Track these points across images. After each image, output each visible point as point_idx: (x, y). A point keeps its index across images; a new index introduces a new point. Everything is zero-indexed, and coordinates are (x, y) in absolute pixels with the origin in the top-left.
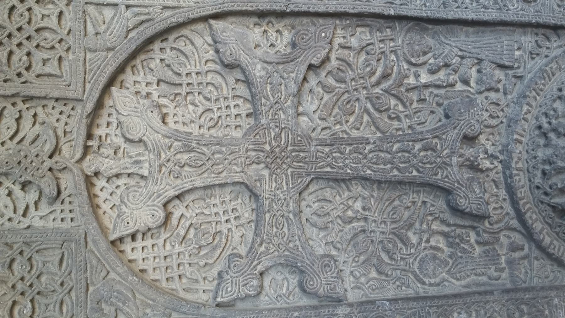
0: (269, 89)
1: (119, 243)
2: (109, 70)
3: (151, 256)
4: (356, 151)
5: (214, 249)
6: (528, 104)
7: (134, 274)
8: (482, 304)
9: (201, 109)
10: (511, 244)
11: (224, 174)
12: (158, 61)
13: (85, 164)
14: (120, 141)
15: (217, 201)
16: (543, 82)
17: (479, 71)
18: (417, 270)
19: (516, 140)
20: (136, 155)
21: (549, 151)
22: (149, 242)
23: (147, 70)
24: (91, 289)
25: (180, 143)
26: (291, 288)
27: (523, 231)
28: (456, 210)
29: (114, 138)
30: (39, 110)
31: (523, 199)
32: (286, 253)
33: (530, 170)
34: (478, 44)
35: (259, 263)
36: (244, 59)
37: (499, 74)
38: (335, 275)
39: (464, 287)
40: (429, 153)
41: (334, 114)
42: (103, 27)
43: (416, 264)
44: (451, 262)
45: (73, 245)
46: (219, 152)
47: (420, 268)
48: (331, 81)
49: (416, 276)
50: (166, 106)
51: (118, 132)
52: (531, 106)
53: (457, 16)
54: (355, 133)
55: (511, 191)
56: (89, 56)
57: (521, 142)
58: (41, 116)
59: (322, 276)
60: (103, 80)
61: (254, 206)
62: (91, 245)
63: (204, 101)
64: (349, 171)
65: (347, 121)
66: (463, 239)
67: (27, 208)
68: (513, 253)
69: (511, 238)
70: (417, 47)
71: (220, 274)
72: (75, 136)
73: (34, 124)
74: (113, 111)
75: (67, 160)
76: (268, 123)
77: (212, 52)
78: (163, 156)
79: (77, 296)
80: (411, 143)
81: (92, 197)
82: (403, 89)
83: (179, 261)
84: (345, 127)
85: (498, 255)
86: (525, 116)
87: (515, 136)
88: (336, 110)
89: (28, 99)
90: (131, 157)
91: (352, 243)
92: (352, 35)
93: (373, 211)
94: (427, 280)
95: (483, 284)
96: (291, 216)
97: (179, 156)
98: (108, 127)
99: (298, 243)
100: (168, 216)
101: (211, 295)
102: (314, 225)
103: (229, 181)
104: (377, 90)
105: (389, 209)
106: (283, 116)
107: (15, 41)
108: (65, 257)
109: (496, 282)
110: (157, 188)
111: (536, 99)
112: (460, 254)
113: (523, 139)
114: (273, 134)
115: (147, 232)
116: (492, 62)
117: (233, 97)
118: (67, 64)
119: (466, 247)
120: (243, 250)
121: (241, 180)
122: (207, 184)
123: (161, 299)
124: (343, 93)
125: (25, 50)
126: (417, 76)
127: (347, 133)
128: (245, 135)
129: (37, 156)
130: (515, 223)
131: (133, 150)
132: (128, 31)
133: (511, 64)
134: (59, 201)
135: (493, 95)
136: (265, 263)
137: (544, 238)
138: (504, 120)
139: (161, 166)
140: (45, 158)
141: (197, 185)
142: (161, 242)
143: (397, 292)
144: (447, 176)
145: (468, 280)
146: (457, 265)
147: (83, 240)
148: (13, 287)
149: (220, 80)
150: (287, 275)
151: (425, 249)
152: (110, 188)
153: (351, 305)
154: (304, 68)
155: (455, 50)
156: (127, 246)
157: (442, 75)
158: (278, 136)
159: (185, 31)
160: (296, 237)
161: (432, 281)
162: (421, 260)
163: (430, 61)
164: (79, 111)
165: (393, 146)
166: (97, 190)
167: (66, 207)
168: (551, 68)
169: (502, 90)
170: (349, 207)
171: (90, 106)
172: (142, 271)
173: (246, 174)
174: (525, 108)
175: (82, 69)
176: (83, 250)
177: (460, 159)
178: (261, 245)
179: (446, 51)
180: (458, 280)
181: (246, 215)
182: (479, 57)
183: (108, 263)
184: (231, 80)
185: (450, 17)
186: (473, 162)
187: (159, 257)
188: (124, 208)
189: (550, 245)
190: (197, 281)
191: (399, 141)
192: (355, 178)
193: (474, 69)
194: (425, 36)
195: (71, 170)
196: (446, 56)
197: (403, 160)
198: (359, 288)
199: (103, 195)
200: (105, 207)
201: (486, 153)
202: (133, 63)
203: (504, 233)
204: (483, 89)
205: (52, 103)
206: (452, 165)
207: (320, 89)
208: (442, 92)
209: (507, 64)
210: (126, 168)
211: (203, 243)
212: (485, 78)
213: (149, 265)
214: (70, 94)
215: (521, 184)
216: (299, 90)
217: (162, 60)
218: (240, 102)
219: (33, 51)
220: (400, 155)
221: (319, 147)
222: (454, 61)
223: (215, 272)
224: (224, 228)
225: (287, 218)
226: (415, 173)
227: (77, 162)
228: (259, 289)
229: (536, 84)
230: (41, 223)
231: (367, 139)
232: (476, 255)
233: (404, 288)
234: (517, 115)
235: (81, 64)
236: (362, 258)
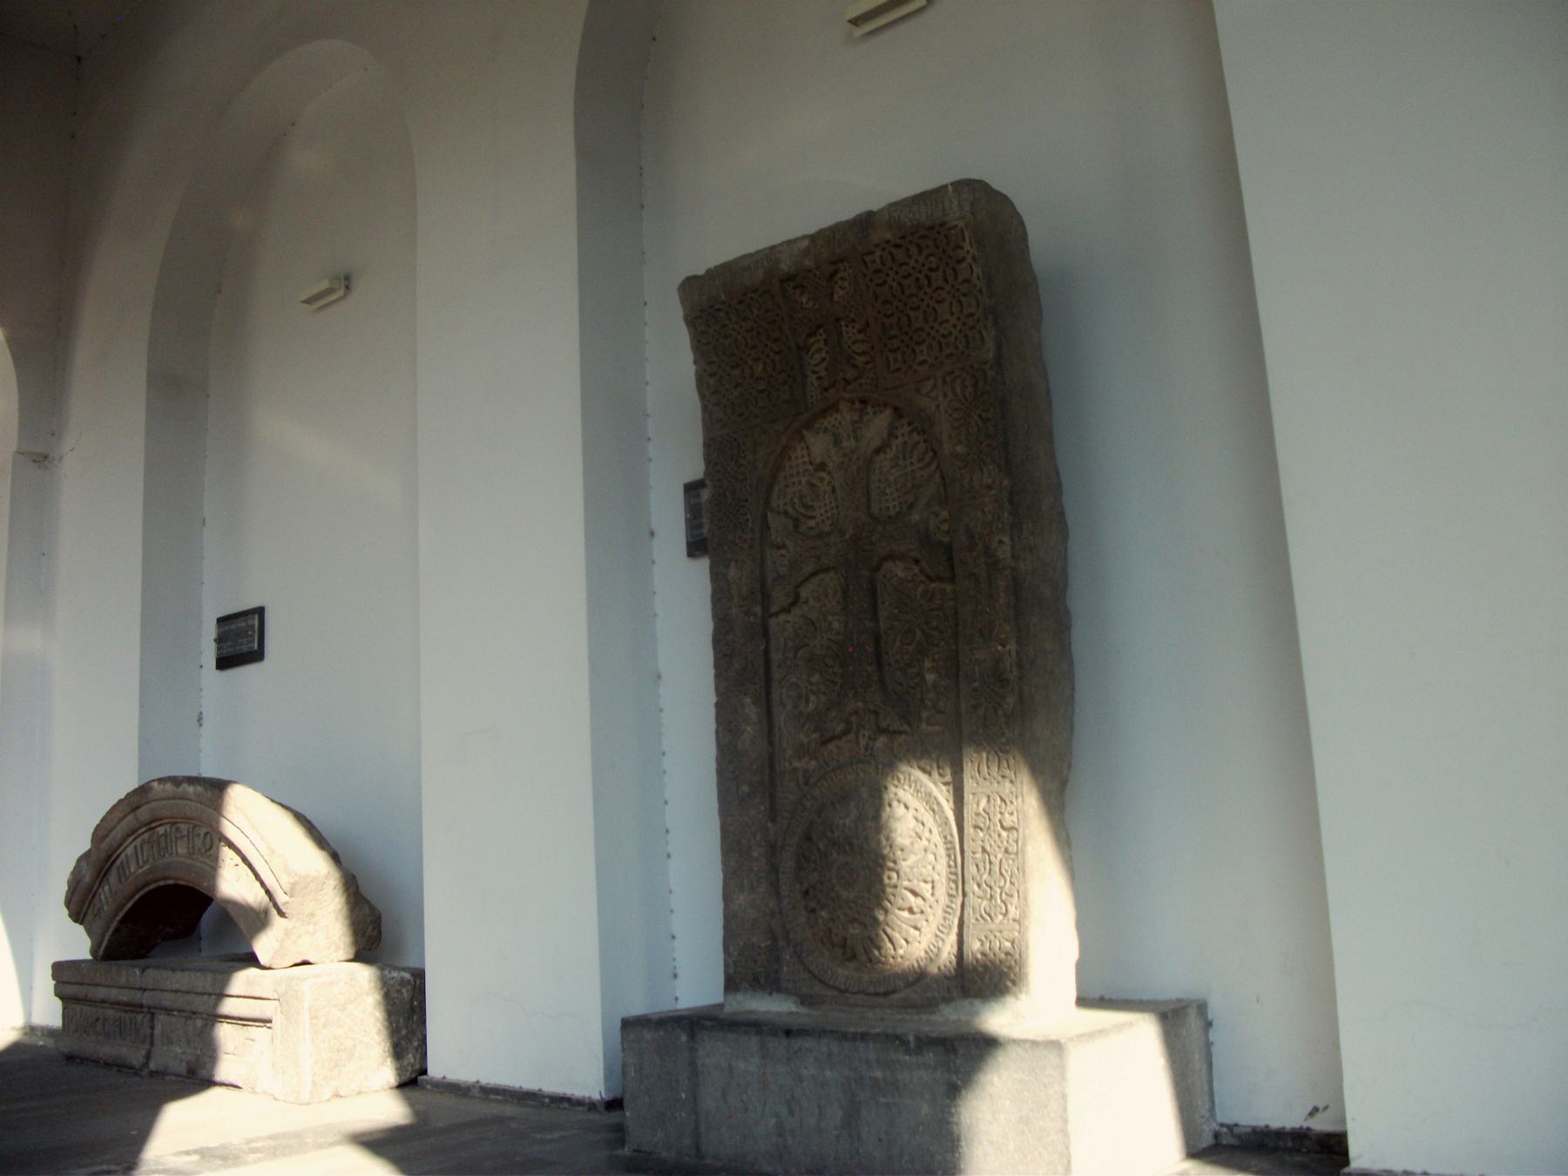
161: (784, 696)
181: (826, 529)
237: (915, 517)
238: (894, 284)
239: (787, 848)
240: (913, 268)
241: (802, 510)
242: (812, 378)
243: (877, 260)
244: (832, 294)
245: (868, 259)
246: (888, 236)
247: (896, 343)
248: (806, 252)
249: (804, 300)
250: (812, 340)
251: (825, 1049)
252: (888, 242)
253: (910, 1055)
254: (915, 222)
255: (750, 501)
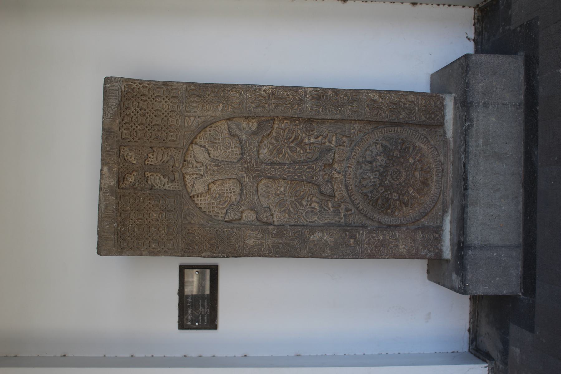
0: (247, 144)
1: (192, 197)
2: (192, 138)
3: (203, 203)
4: (280, 168)
5: (226, 202)
6: (355, 152)
7: (197, 208)
8: (328, 230)
9: (223, 151)
10: (346, 208)
11: (230, 175)
12: (208, 134)
13: (183, 170)
14: (195, 162)
15: (227, 185)
16: (362, 143)
17: (336, 137)
18: (305, 217)
19: (349, 166)
20: (200, 167)
21: (361, 171)
22: (203, 198)
23: (204, 137)
24: (183, 211)
25: (214, 164)
26: (253, 219)
27: (351, 204)
28: (321, 193)
29: (192, 161)
30: (170, 151)
31: (351, 190)
32: (251, 205)
33: (354, 179)
34: (335, 128)
35: (241, 208)
36: (239, 133)
37: (344, 139)
38: (269, 214)
39: (324, 224)
40: (310, 170)
41: (274, 154)
42: (190, 124)
43: (304, 214)
44: (319, 214)
45: (178, 196)
46: (229, 167)
47: (306, 215)
48: (273, 141)
49: (304, 218)
50: (211, 150)
51: (194, 159)
52: (357, 153)
53: (323, 118)
54: (282, 161)
55: (346, 187)
56: (185, 133)
57: (351, 167)
58: (170, 153)
59: (264, 215)
60: (190, 141)
61: (241, 188)
62: (184, 197)
63: (224, 148)
64: (277, 176)
65: (278, 157)
66: (325, 205)
67: (164, 184)
68: (347, 212)
69: (346, 206)
70: (309, 129)
71: (227, 211)
72: (180, 160)
73: (167, 156)
74: (192, 152)
75: (178, 168)
76: (247, 157)
77: (227, 130)
78: (208, 168)
79: (179, 213)
80: (302, 166)
81: (185, 181)
82: (303, 144)
83: (213, 205)
84: (278, 159)
85: (340, 212)
86: (353, 157)
87: (348, 165)
88: (275, 152)
89: (167, 148)
90: (197, 168)
91: (278, 204)
92: (282, 124)
93: (288, 192)
94: (308, 220)
95: (332, 223)
96: (254, 192)
97: (214, 168)
98: (190, 157)
99: (256, 202)
100: (209, 189)
101: (223, 218)
102: (263, 196)
103: (231, 178)
104: (292, 145)
105: (294, 191)
106: (252, 154)
107: (163, 130)
108: (176, 200)
109: (338, 223)
110: (206, 179)
111: (358, 150)
112: (323, 211)
113: (352, 166)
114: (248, 161)
115: (202, 194)
116: (341, 135)
117: (234, 147)
118: (178, 136)
119: (326, 208)
120: (235, 203)
121: (235, 178)
122: (223, 178)
123: (206, 217)
124: (278, 146)
125: (166, 132)
126: (309, 140)
127: (279, 162)
128: (238, 161)
129: (168, 167)
130: (348, 200)
131: (198, 165)
132: (199, 125)
133: (349, 135)
134: (174, 182)
135: (342, 147)
136: (244, 208)
137: (358, 207)
138: (345, 158)
139: (207, 171)
140: (171, 167)
141: (220, 178)
142: (206, 198)
143: (295, 223)
144: (317, 180)
145: (326, 221)
146: (321, 215)
147: (181, 195)
148: (160, 208)
149: (230, 141)
150: (252, 214)
151: (308, 208)
152: (191, 179)
153: (274, 226)
154: (261, 137)
155: (325, 130)
156: (196, 199)
157: (320, 139)
158: (250, 162)
159: (218, 123)
160: (255, 200)
161: (310, 221)
162: (306, 212)
163: (315, 134)
164: (182, 152)
165: (295, 167)
166: (186, 179)
167: (177, 184)
168: (366, 138)
169: (346, 146)
170: (278, 190)
171: (185, 150)
172: (200, 208)
173: (237, 175)
174: (353, 154)
175: (183, 137)
176: (181, 198)
177: (324, 173)
178: (242, 201)
179: (321, 130)
180: (321, 221)
181: (238, 191)
182: (335, 132)
183: (189, 203)
184: (234, 141)
185: (320, 118)
186: (329, 175)
187: (206, 203)
188: (194, 185)
189: (362, 210)
190: (219, 213)
191: (297, 165)
192: (280, 179)
193: (334, 137)
194: (313, 124)
195: (178, 172)
196: (321, 132)
197: (299, 172)
198: (280, 221)
199: (188, 181)
200: (189, 185)
201: (335, 171)
202: (200, 135)
203: (343, 204)
204: (337, 145)
205: (174, 149)
206: (319, 176)
207: (268, 144)
208: (319, 146)
209: (347, 135)
210: (196, 172)
211: (221, 200)
212: (337, 141)
213: (203, 206)
214: (179, 146)
215: (350, 184)
216: (259, 145)
217: (210, 134)
218: (237, 149)
219: (169, 132)
220: (298, 170)
221: (266, 166)
222: (324, 134)
223: (225, 210)
224: (229, 195)
225: (253, 192)
226: (304, 178)
227: (180, 169)
228: (240, 217)
229: (359, 144)
230: (169, 189)
231: (285, 164)
232: (330, 212)
233: (299, 223)
234: (349, 156)
235: (183, 136)
236: (282, 210)
237: (244, 137)
238: (139, 127)
239: (379, 220)
240: (135, 115)
241: (227, 203)
242: (167, 187)
243: (126, 132)
244: (133, 164)
245: (124, 136)
246: (118, 122)
247: (164, 134)
248: (110, 169)
249: (130, 180)
250: (149, 182)
251: (472, 169)
252: (120, 123)
253: (473, 125)
254: (117, 106)
255: (218, 229)
